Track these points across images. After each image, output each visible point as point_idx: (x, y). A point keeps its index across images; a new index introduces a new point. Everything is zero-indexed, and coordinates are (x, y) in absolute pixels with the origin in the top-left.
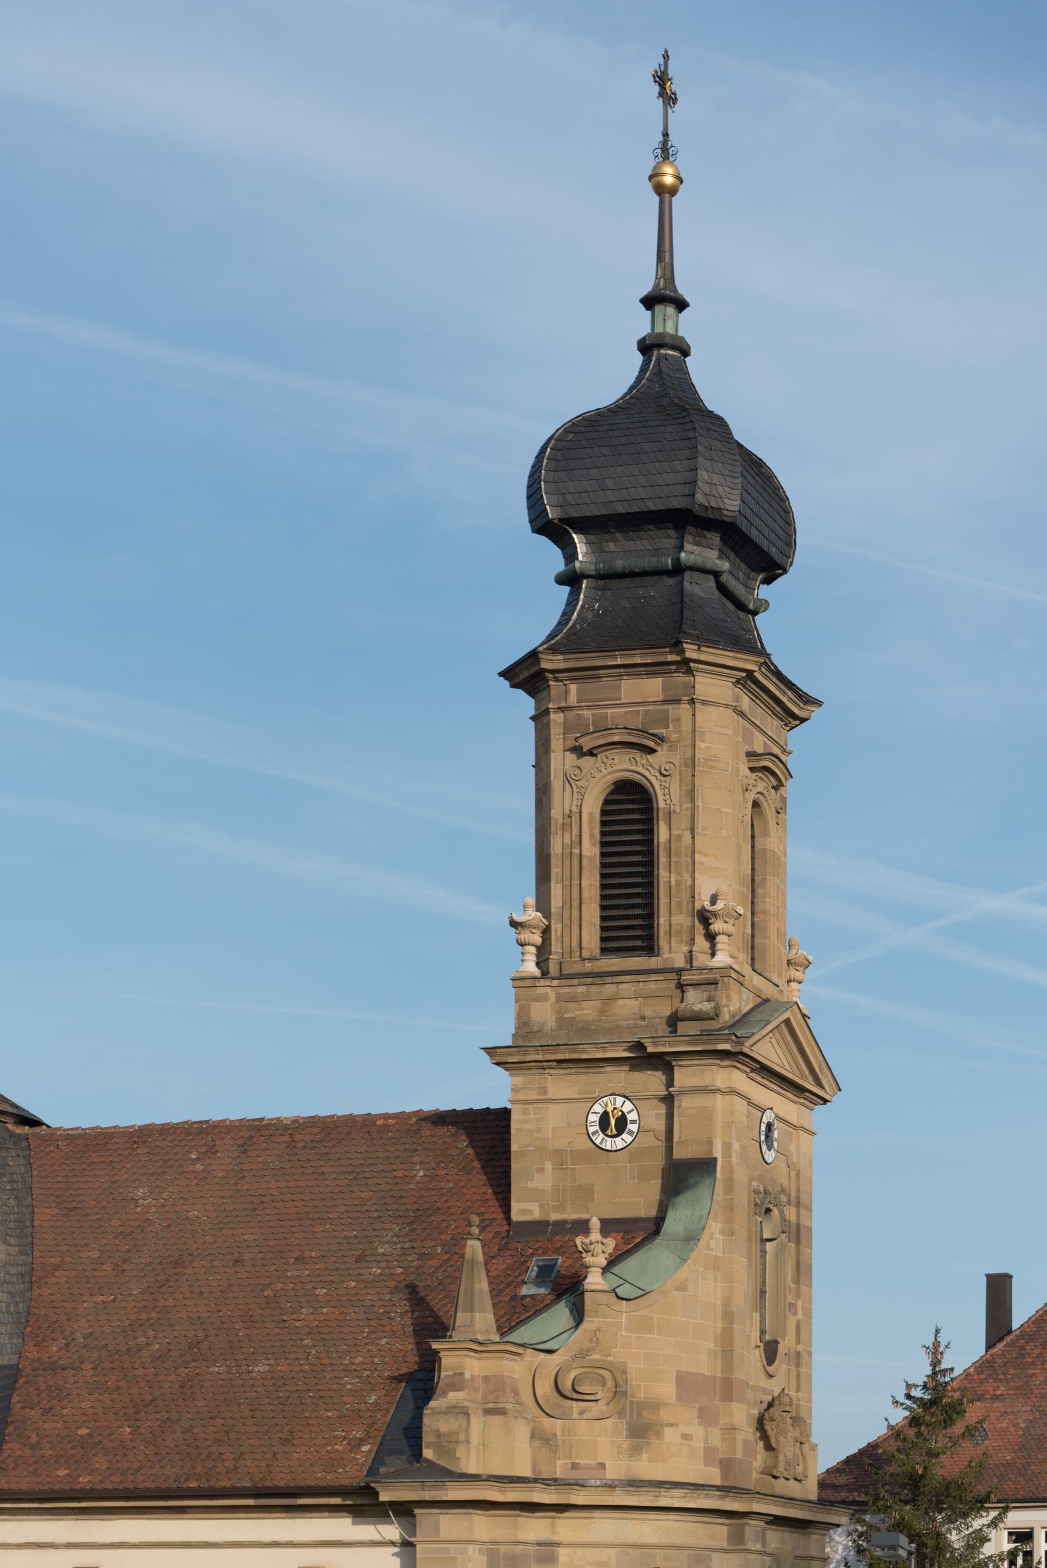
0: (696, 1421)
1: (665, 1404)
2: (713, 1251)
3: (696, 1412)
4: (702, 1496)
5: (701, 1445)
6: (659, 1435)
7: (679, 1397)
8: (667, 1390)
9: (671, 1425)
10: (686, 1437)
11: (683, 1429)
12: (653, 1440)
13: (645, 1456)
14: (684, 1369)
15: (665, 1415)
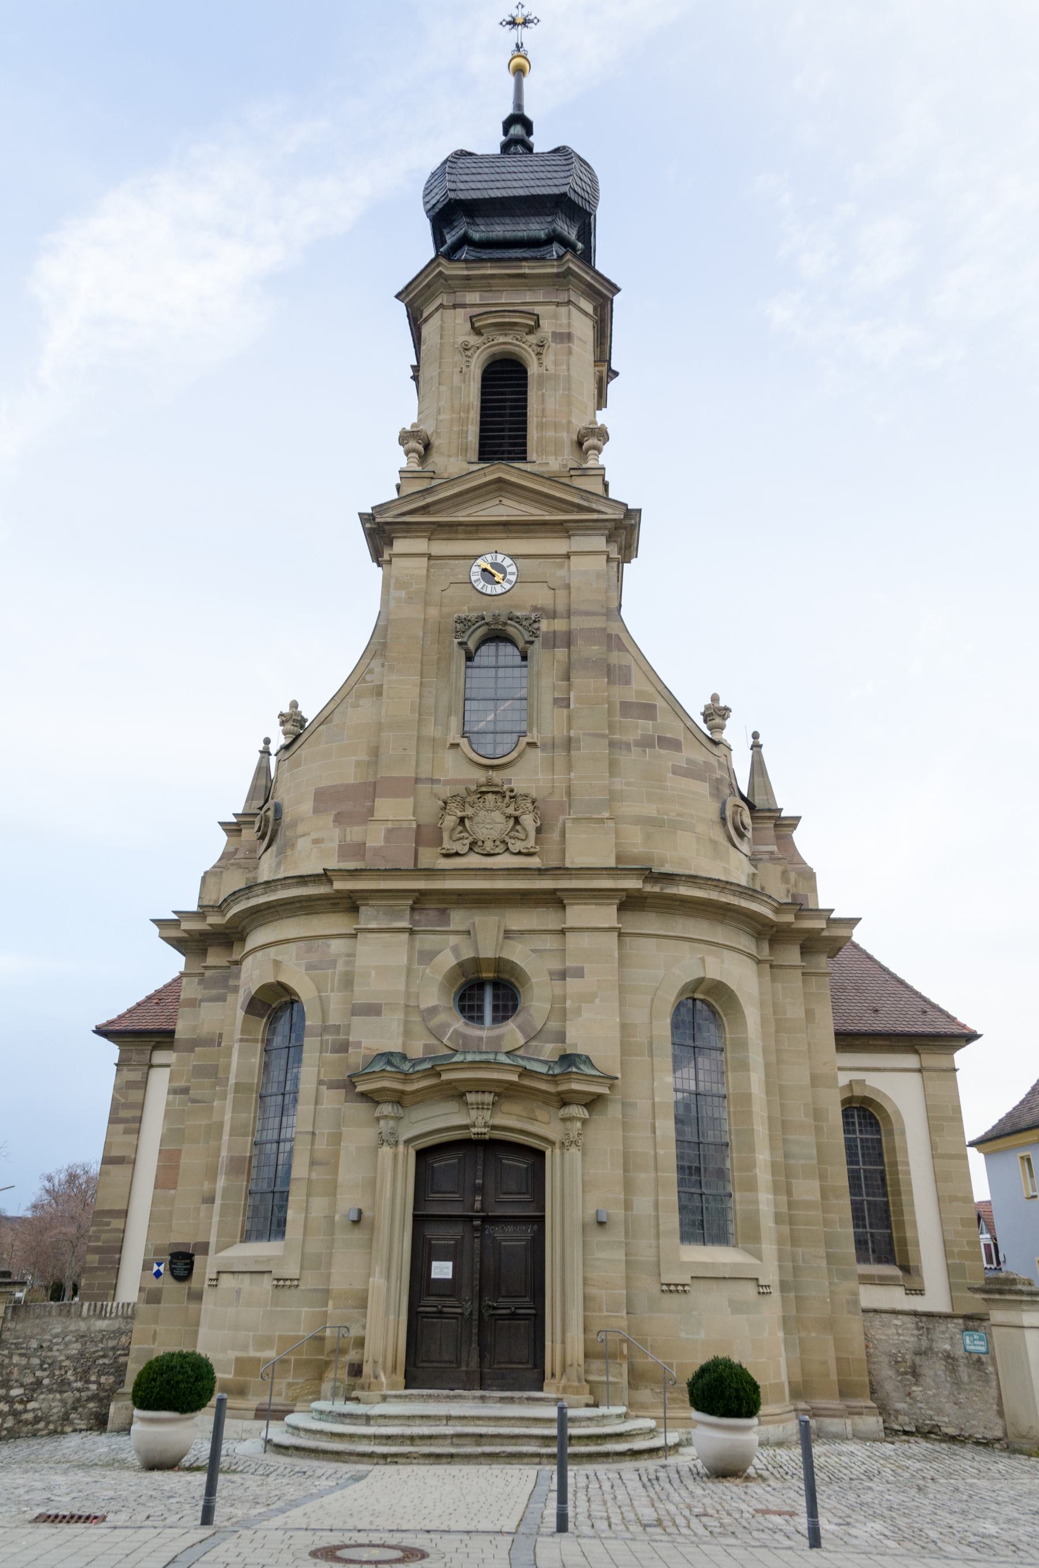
0: (331, 824)
1: (302, 820)
2: (372, 681)
3: (332, 818)
4: (279, 887)
5: (335, 845)
6: (293, 846)
7: (316, 810)
8: (307, 807)
9: (303, 836)
10: (316, 841)
11: (314, 836)
12: (289, 852)
13: (282, 868)
14: (324, 783)
15: (301, 829)
